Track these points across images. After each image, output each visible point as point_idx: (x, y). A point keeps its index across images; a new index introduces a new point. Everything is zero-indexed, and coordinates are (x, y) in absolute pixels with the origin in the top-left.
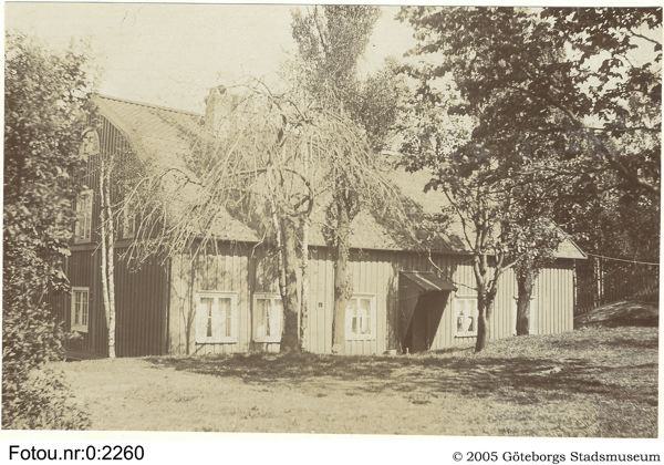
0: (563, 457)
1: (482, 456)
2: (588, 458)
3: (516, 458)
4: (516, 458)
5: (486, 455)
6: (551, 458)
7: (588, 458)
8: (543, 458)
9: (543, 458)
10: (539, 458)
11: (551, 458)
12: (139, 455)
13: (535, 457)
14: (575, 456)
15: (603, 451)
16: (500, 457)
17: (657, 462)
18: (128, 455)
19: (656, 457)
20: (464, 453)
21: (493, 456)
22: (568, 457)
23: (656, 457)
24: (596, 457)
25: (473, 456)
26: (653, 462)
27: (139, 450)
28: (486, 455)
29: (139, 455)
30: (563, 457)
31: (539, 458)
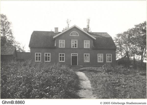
0: (125, 103)
1: (107, 103)
2: (130, 103)
3: (114, 103)
4: (114, 103)
6: (122, 103)
7: (130, 103)
8: (120, 103)
9: (120, 103)
10: (119, 103)
11: (122, 103)
12: (23, 103)
13: (118, 103)
15: (134, 102)
17: (145, 104)
18: (21, 103)
19: (145, 103)
21: (109, 103)
22: (126, 103)
24: (132, 103)
27: (23, 102)
29: (23, 103)
30: (125, 103)
31: (119, 103)
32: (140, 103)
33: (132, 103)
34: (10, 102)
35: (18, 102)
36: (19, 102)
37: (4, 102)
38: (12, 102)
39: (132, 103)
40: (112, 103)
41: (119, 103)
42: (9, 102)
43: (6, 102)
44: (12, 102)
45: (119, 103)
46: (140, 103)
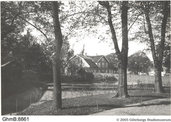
1: (124, 120)
2: (152, 120)
3: (133, 120)
4: (133, 120)
5: (125, 120)
6: (142, 120)
7: (152, 120)
8: (140, 120)
9: (140, 120)
11: (142, 120)
13: (138, 120)
14: (149, 120)
16: (129, 120)
17: (170, 121)
18: (25, 120)
19: (169, 120)
20: (120, 119)
21: (127, 120)
22: (147, 120)
23: (169, 120)
24: (154, 120)
25: (122, 120)
26: (169, 121)
28: (125, 120)
32: (163, 120)
33: (154, 120)
34: (12, 119)
35: (21, 119)
36: (22, 118)
37: (5, 118)
38: (14, 119)
39: (154, 120)
40: (131, 120)
41: (138, 120)
42: (10, 119)
43: (8, 119)
44: (14, 119)
45: (138, 120)
46: (163, 120)
